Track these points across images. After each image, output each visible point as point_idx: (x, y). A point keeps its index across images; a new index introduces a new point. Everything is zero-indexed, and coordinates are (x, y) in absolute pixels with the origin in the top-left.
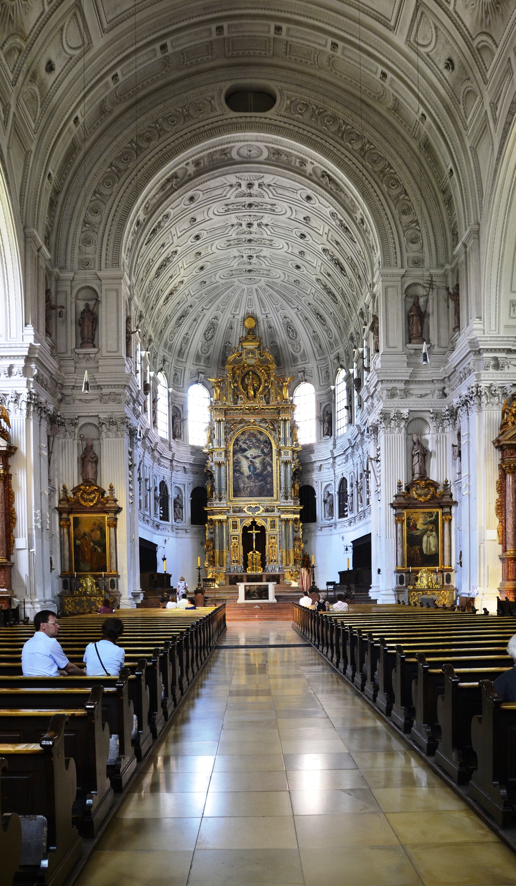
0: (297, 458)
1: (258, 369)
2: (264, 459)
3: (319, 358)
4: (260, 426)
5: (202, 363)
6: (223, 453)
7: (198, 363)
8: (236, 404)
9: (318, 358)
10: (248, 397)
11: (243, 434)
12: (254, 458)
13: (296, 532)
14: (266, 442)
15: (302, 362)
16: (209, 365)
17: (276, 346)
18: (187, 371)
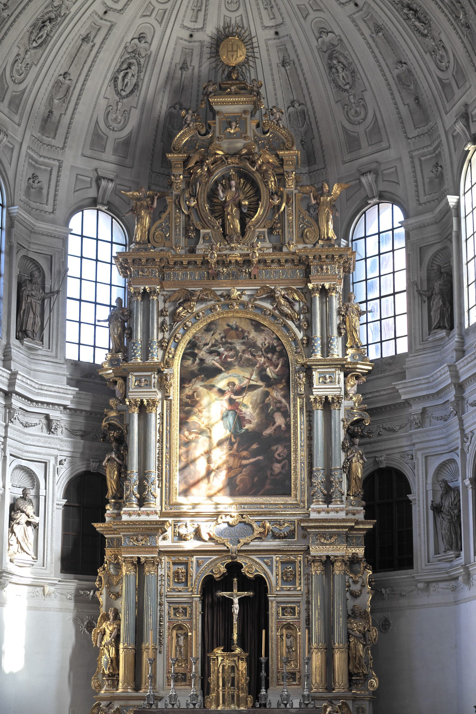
0: (358, 392)
1: (253, 163)
2: (266, 394)
3: (416, 133)
4: (256, 307)
5: (109, 155)
6: (155, 378)
7: (96, 155)
8: (192, 251)
9: (413, 133)
10: (224, 235)
11: (208, 329)
12: (240, 391)
13: (355, 595)
14: (271, 349)
15: (370, 149)
16: (128, 162)
17: (303, 114)
18: (65, 173)
